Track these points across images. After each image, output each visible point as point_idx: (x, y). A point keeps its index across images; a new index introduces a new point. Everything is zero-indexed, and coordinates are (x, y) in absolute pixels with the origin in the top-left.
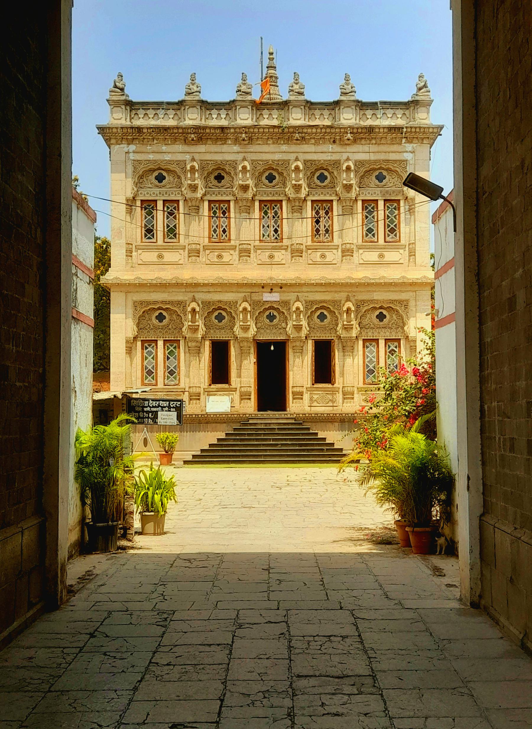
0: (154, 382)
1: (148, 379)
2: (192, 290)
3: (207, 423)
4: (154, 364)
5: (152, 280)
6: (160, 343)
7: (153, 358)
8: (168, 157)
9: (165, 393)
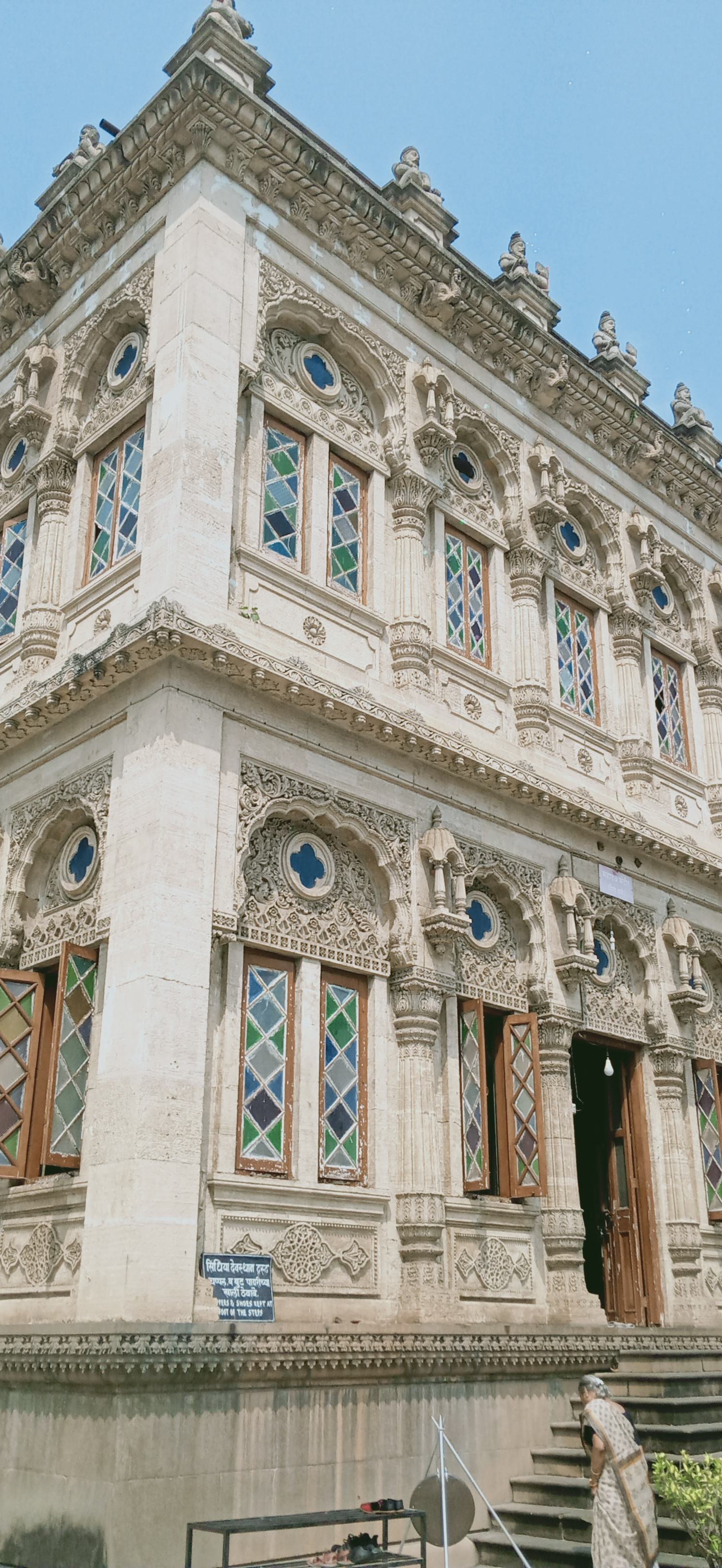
0: (278, 1158)
1: (255, 1141)
2: (435, 787)
3: (492, 1378)
4: (282, 1067)
5: (344, 692)
6: (310, 972)
7: (277, 1039)
8: (364, 318)
9: (318, 1220)
